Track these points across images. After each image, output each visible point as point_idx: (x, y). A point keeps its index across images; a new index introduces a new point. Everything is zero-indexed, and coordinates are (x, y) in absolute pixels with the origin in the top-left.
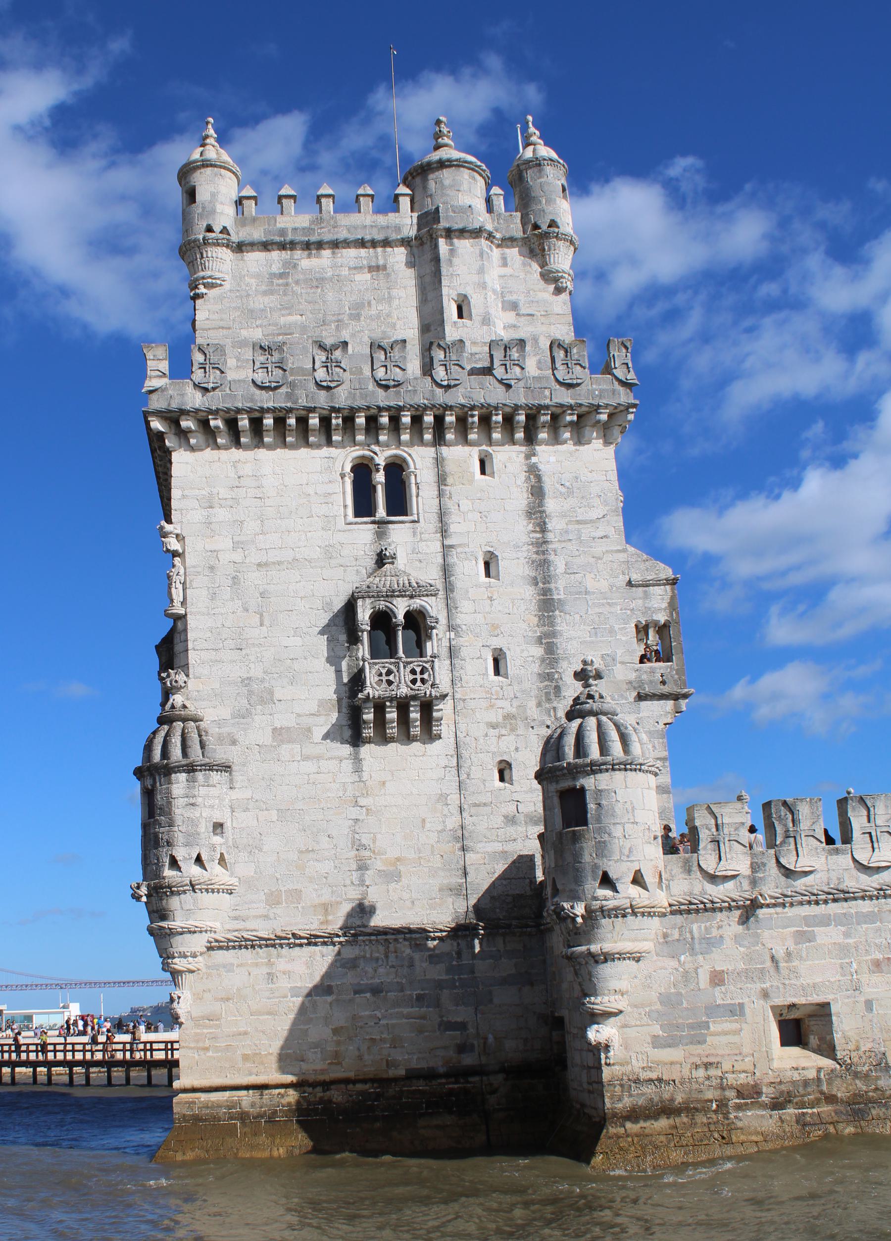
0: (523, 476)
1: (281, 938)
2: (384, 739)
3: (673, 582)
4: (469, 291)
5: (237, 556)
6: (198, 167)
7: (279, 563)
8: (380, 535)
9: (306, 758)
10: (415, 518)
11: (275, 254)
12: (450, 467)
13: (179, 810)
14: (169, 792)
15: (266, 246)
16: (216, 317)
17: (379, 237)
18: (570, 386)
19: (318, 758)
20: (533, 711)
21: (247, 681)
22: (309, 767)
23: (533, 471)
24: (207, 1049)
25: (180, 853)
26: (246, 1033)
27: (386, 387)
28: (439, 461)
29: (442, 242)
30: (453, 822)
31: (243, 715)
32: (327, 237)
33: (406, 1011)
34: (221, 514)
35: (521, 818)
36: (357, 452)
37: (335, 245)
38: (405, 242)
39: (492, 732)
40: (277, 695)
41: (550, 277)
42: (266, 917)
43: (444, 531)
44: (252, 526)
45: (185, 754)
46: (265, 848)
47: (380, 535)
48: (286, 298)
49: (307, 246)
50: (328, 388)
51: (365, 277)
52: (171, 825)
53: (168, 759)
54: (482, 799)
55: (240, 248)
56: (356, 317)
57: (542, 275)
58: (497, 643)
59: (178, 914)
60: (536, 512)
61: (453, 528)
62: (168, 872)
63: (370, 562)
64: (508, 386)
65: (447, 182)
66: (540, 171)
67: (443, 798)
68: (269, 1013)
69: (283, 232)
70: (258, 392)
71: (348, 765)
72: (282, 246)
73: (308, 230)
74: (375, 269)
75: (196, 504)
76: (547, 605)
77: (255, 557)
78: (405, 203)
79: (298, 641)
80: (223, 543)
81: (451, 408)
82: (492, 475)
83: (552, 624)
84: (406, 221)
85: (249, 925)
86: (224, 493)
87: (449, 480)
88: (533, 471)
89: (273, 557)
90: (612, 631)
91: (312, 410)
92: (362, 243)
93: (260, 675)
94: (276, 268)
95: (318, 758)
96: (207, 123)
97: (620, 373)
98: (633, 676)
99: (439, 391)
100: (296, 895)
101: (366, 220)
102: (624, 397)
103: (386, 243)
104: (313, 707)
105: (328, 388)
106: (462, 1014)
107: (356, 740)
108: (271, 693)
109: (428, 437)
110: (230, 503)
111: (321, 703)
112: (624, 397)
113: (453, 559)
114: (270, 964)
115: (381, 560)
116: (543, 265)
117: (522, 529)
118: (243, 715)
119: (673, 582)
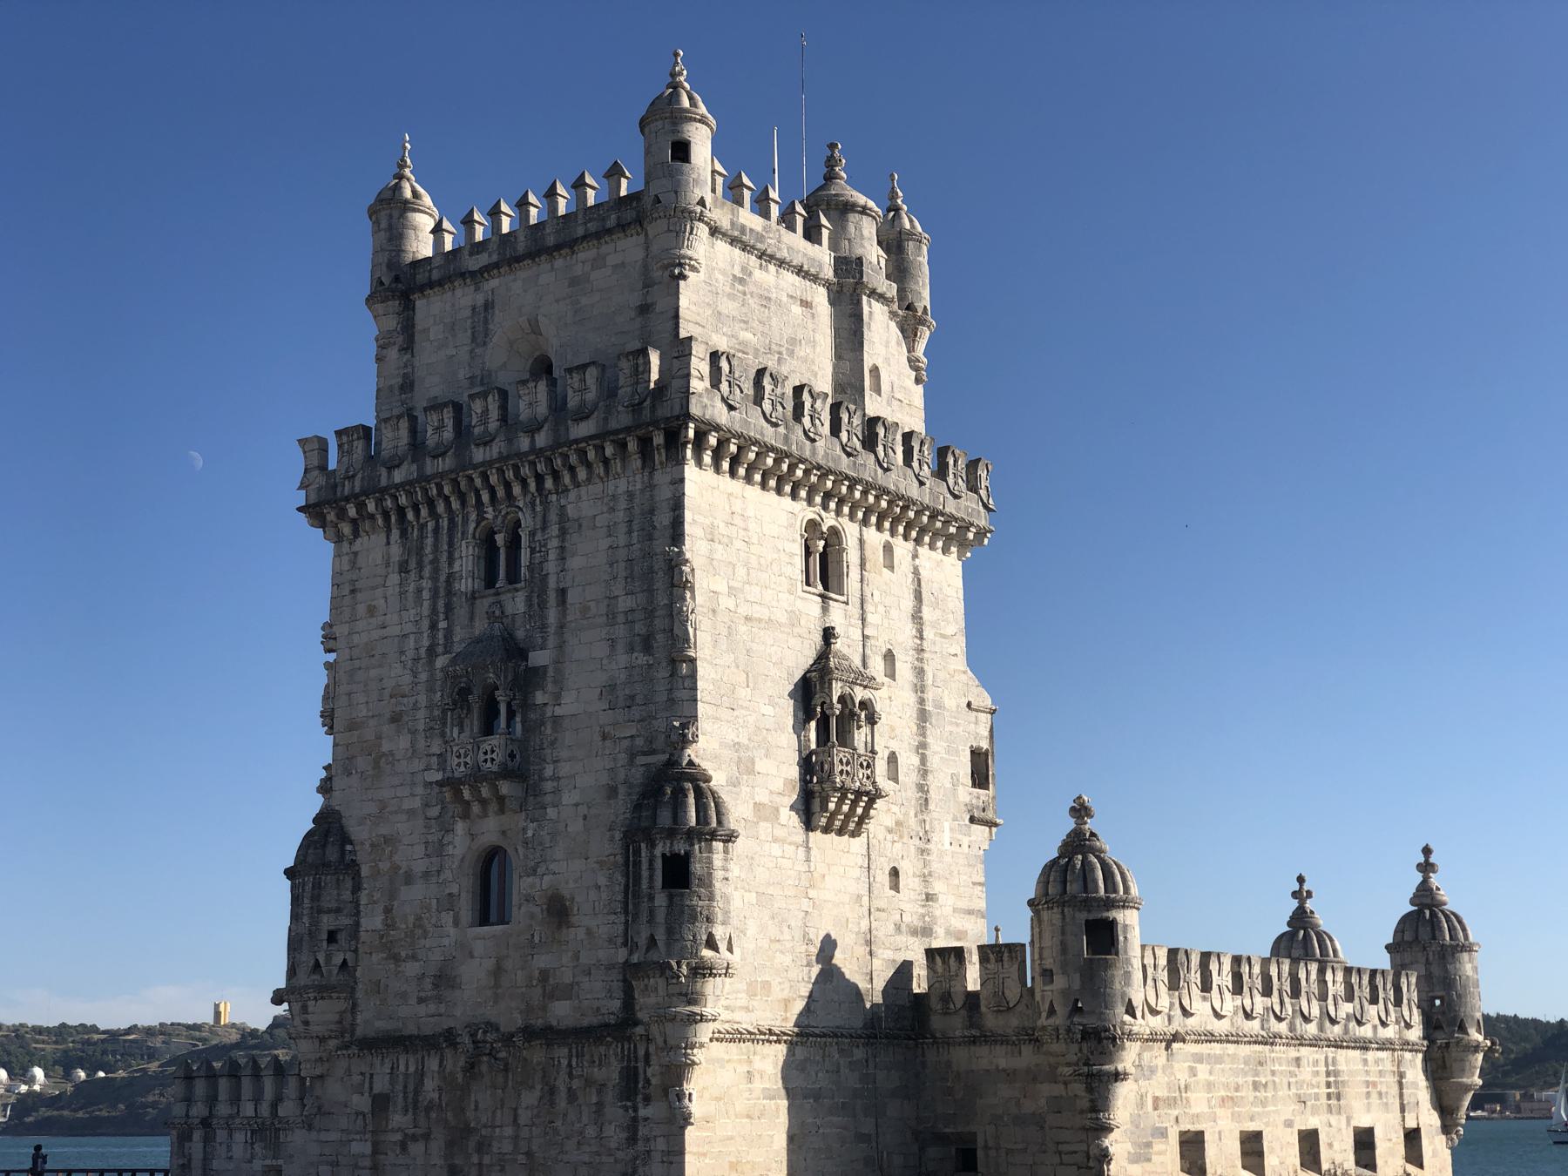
0: (911, 576)
1: (761, 1033)
2: (826, 830)
3: (993, 712)
4: (880, 366)
5: (731, 603)
6: (695, 120)
7: (760, 620)
8: (825, 609)
9: (775, 840)
10: (843, 598)
11: (737, 251)
12: (868, 553)
13: (718, 885)
14: (710, 862)
15: (733, 241)
16: (693, 308)
17: (813, 271)
18: (956, 497)
19: (783, 841)
20: (912, 822)
21: (737, 746)
22: (776, 849)
23: (916, 572)
24: (704, 1155)
25: (719, 932)
26: (731, 1138)
27: (849, 455)
28: (861, 541)
29: (865, 298)
30: (864, 924)
31: (734, 783)
32: (778, 255)
33: (835, 1119)
34: (720, 552)
35: (904, 928)
36: (810, 513)
37: (781, 263)
38: (828, 285)
39: (889, 837)
40: (758, 768)
41: (913, 363)
42: (747, 1009)
43: (863, 620)
44: (741, 572)
45: (719, 822)
46: (749, 933)
47: (825, 609)
48: (744, 310)
49: (762, 255)
50: (813, 441)
51: (797, 309)
52: (711, 898)
53: (708, 824)
54: (882, 904)
55: (715, 231)
56: (791, 353)
57: (909, 360)
58: (894, 746)
59: (710, 999)
60: (917, 617)
61: (870, 618)
62: (707, 953)
63: (818, 638)
64: (922, 484)
65: (866, 233)
66: (920, 248)
67: (859, 897)
68: (748, 1116)
69: (743, 229)
70: (765, 424)
71: (801, 849)
72: (745, 247)
73: (761, 238)
74: (806, 304)
75: (699, 532)
76: (923, 716)
77: (744, 610)
78: (825, 233)
79: (768, 710)
80: (722, 587)
81: (888, 493)
82: (891, 567)
83: (924, 735)
84: (822, 256)
85: (737, 1016)
86: (722, 529)
87: (868, 566)
88: (916, 572)
89: (757, 611)
90: (957, 751)
91: (802, 460)
92: (799, 271)
93: (746, 742)
94: (737, 272)
95: (783, 841)
96: (676, 55)
97: (983, 493)
98: (967, 799)
99: (880, 471)
100: (766, 985)
101: (793, 243)
102: (982, 521)
103: (815, 279)
104: (778, 785)
105: (813, 441)
106: (868, 1127)
107: (809, 825)
108: (753, 763)
109: (860, 515)
110: (725, 540)
111: (787, 782)
112: (982, 521)
113: (868, 652)
114: (749, 1061)
115: (828, 634)
116: (910, 350)
117: (909, 629)
118: (734, 783)
119: (993, 712)
